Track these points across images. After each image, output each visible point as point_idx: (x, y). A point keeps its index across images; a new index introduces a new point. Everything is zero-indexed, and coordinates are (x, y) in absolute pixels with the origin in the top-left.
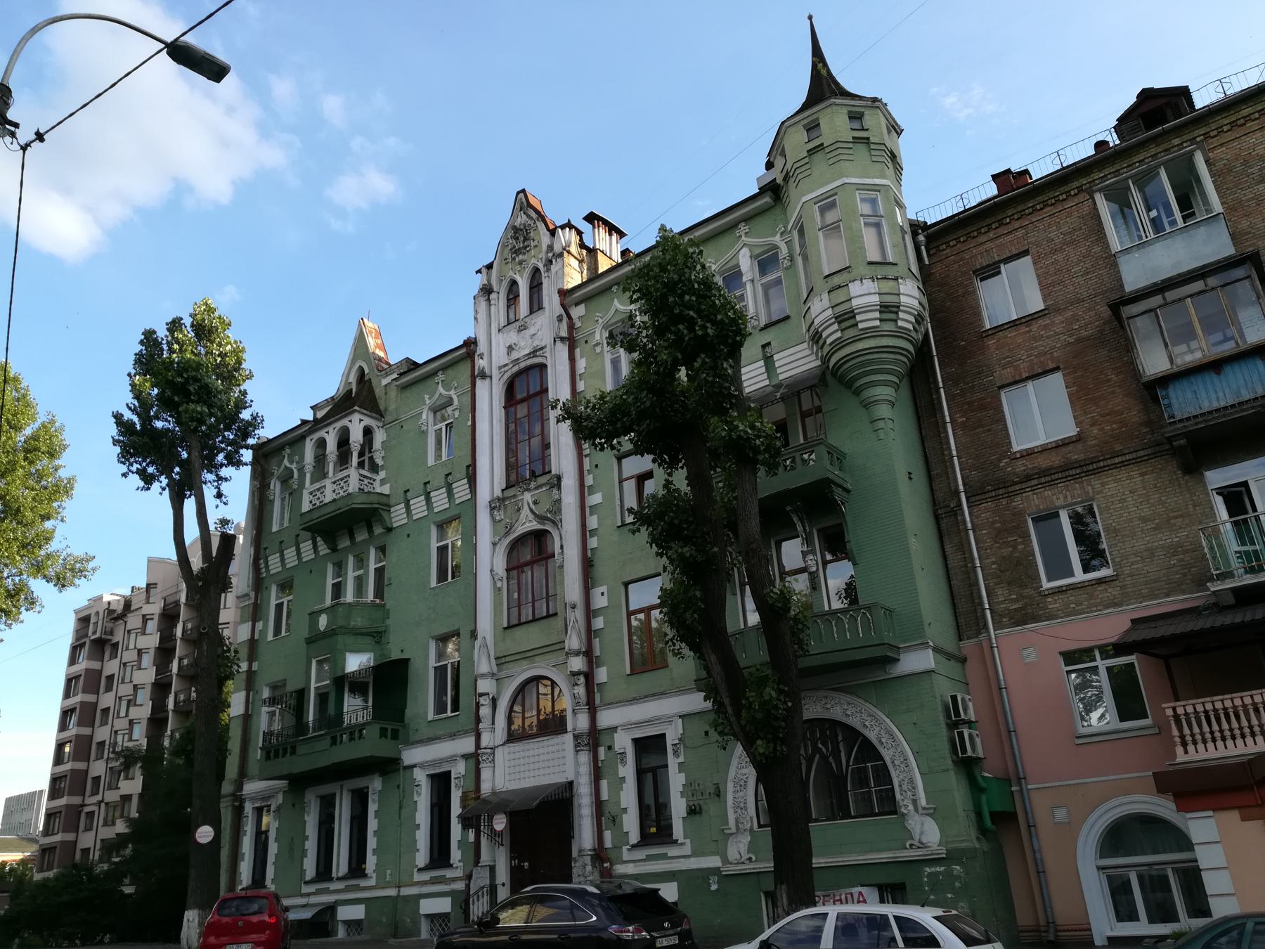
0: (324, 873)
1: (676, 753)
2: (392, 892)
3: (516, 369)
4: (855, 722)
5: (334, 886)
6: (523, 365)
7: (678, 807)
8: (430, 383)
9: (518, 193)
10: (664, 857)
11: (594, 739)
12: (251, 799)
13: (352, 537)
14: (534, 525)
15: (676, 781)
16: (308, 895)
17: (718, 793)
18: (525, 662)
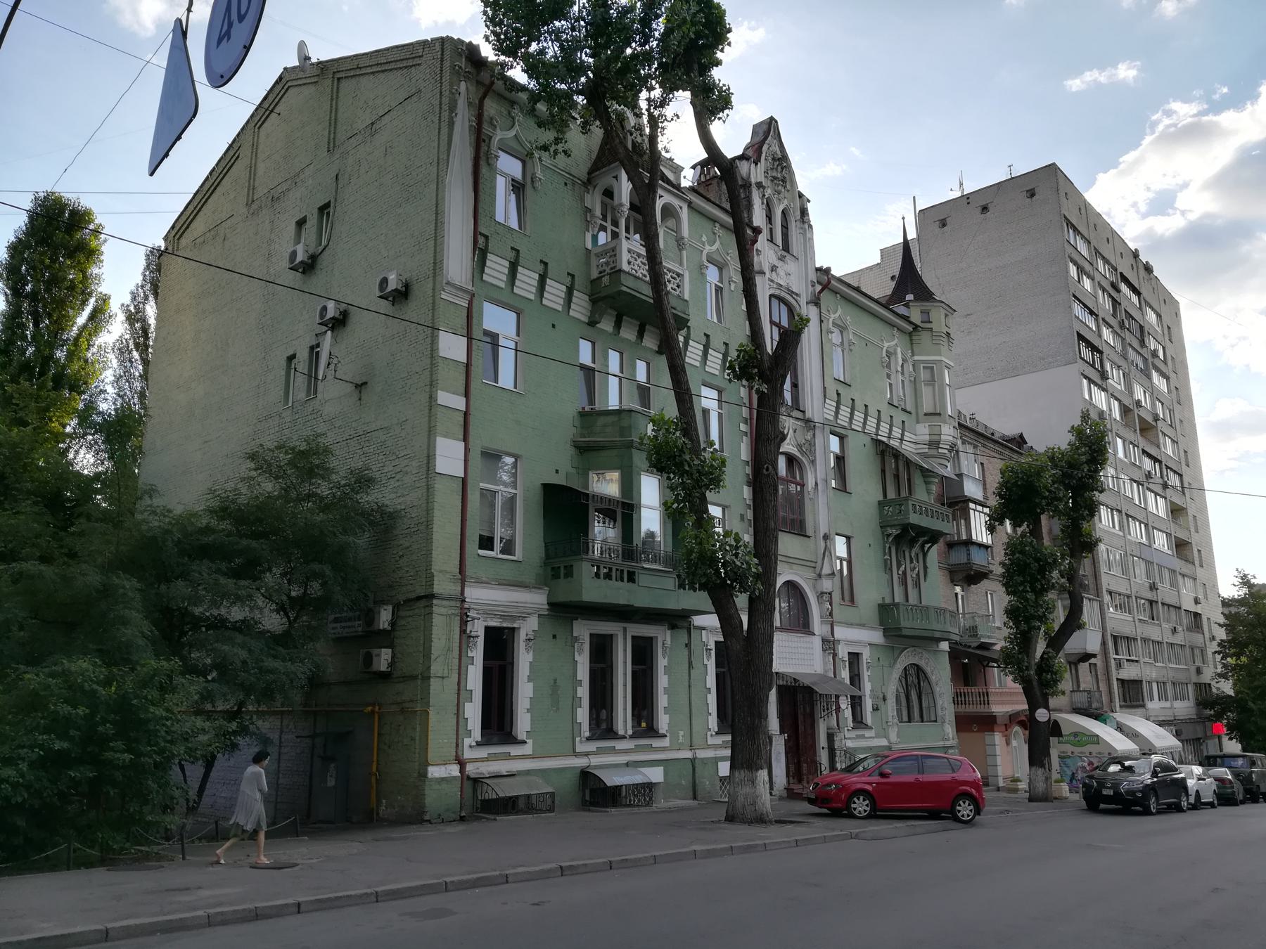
0: (603, 728)
1: (868, 668)
2: (688, 754)
3: (778, 292)
4: (928, 670)
5: (620, 745)
6: (783, 294)
7: (868, 704)
8: (708, 225)
9: (772, 119)
10: (863, 737)
11: (830, 645)
12: (488, 614)
13: (618, 325)
14: (793, 450)
15: (867, 686)
16: (587, 754)
17: (884, 699)
18: (786, 565)
